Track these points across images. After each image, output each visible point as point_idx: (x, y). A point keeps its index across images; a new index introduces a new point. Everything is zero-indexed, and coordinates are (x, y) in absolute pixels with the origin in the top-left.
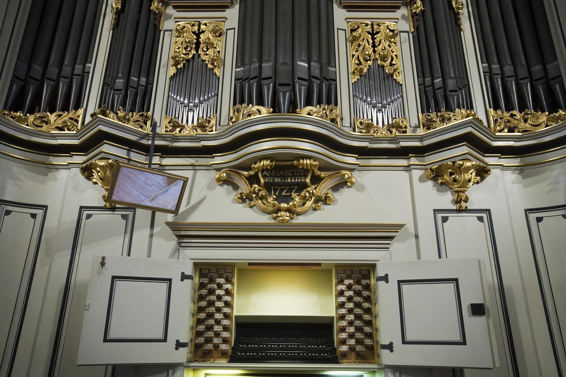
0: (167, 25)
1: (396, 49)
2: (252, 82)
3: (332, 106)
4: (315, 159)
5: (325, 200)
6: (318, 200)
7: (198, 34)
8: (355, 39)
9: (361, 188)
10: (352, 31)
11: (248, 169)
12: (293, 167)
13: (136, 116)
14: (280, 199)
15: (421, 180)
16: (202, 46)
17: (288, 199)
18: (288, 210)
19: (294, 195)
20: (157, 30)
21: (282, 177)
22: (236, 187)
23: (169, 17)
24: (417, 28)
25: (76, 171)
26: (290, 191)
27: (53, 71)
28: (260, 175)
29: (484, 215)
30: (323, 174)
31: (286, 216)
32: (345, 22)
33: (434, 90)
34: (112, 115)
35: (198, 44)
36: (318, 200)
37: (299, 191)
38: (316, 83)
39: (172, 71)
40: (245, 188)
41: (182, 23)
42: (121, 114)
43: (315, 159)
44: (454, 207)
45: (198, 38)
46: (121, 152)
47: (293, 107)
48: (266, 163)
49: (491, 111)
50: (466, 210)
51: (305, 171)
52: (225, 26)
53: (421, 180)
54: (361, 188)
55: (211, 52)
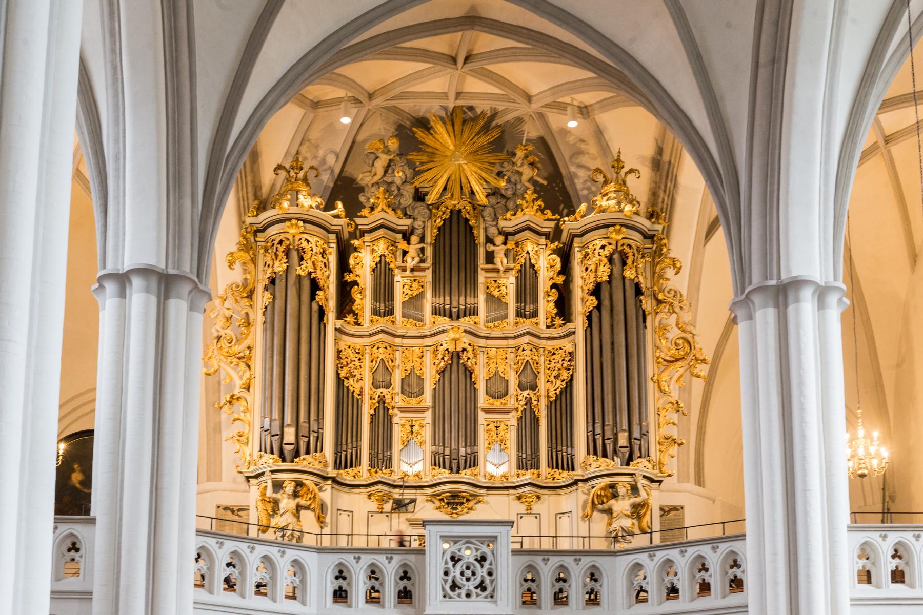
0: (395, 420)
1: (508, 435)
2: (440, 455)
3: (475, 468)
4: (468, 493)
5: (471, 509)
6: (469, 509)
7: (412, 426)
8: (488, 431)
9: (487, 503)
10: (488, 425)
11: (439, 495)
12: (458, 495)
13: (388, 470)
14: (453, 509)
15: (513, 500)
16: (414, 434)
17: (456, 509)
18: (456, 513)
19: (458, 507)
20: (391, 422)
21: (454, 499)
22: (434, 503)
23: (397, 415)
24: (518, 424)
25: (366, 496)
26: (457, 505)
27: (344, 448)
28: (445, 499)
29: (538, 516)
30: (470, 498)
31: (455, 516)
32: (484, 420)
33: (522, 459)
34: (381, 472)
35: (412, 432)
36: (469, 509)
37: (461, 506)
38: (469, 456)
39: (401, 447)
40: (438, 503)
41: (403, 421)
42: (384, 471)
43: (468, 493)
44: (526, 512)
45: (412, 429)
46: (386, 488)
47: (458, 472)
48: (448, 494)
49: (547, 468)
50: (531, 514)
51: (463, 497)
52: (424, 422)
53: (513, 500)
54: (487, 503)
55: (419, 436)
